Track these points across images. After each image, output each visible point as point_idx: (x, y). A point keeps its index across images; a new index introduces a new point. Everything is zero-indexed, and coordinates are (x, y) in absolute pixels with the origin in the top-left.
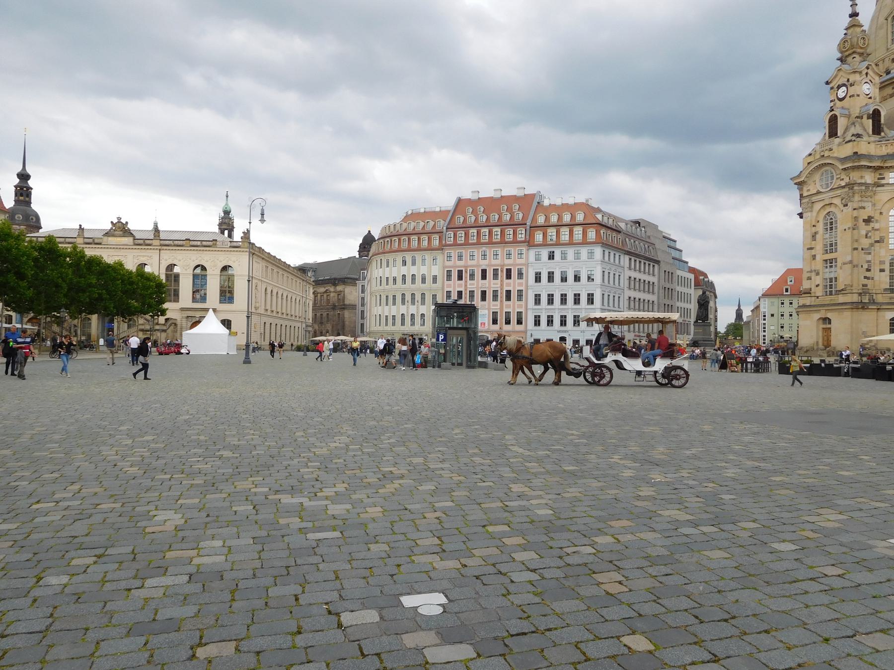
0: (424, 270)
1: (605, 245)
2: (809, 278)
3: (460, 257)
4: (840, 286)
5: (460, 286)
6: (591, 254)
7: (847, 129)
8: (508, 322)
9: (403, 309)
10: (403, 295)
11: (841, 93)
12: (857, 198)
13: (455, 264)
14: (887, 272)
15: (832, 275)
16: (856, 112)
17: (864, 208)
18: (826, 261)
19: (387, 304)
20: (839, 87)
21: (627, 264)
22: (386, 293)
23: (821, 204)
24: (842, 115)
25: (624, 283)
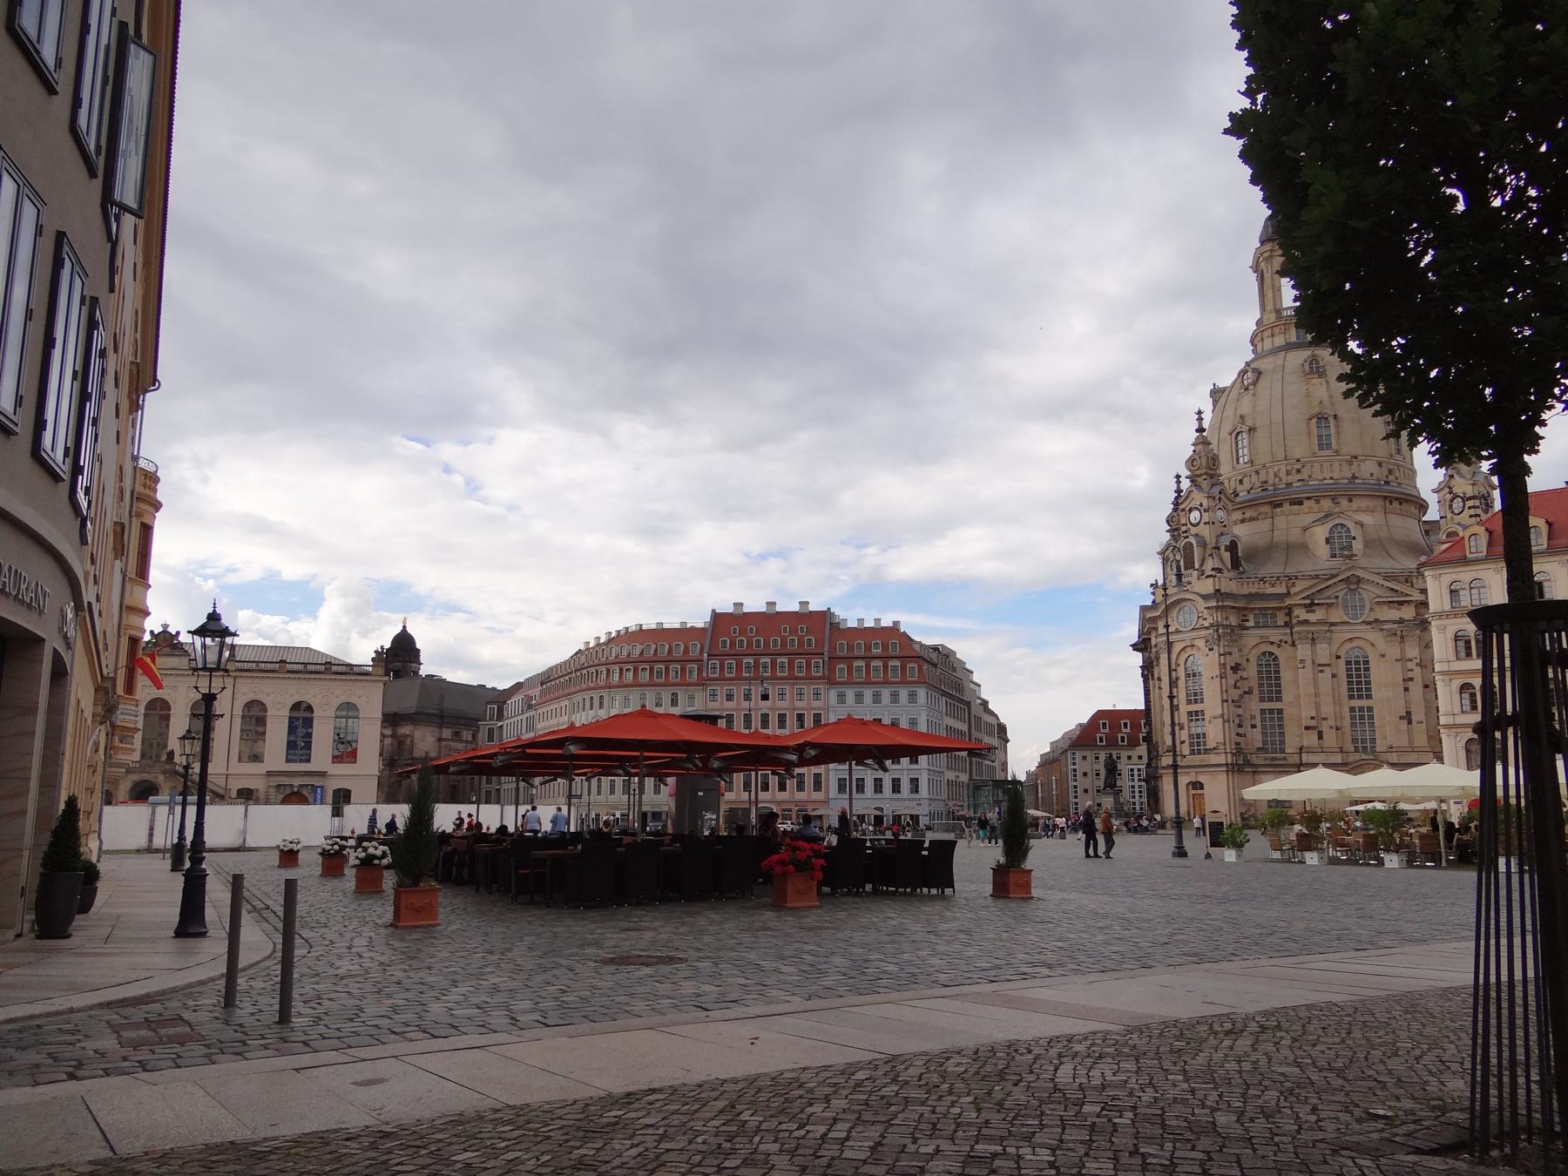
4: (1210, 745)
6: (913, 697)
11: (1195, 516)
14: (1259, 729)
15: (1199, 731)
16: (1211, 541)
18: (1190, 713)
23: (1182, 645)
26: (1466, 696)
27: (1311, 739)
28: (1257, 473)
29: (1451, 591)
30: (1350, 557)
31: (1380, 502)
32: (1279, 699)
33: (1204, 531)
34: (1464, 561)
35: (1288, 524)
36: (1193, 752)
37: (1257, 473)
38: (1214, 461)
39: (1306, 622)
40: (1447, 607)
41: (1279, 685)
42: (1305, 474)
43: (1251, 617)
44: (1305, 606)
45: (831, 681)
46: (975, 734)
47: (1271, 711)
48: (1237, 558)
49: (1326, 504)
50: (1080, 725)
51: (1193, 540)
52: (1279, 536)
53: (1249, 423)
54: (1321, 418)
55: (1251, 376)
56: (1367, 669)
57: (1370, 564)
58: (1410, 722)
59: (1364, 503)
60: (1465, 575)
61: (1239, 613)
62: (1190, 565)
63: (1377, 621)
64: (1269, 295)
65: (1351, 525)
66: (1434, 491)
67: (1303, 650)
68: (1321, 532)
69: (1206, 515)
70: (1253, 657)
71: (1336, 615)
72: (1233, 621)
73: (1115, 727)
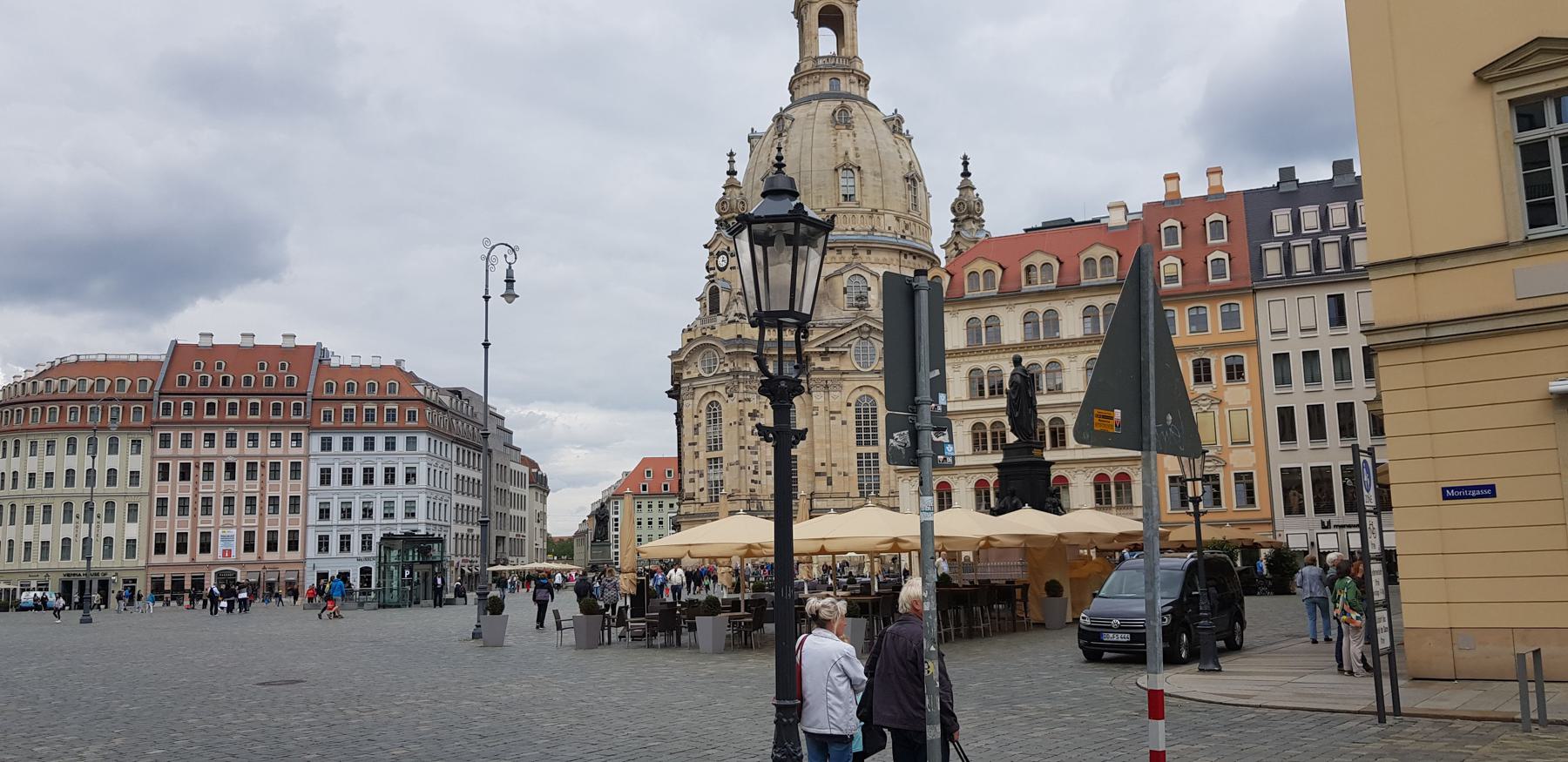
0: (113, 461)
1: (430, 430)
2: (692, 481)
3: (186, 442)
5: (186, 489)
6: (411, 443)
8: (272, 546)
9: (67, 530)
10: (68, 505)
11: (722, 261)
12: (742, 388)
13: (176, 453)
15: (718, 478)
19: (29, 522)
20: (719, 254)
22: (28, 502)
24: (725, 289)
27: (821, 485)
31: (896, 256)
44: (821, 354)
45: (312, 429)
49: (847, 255)
56: (875, 417)
62: (714, 309)
65: (867, 276)
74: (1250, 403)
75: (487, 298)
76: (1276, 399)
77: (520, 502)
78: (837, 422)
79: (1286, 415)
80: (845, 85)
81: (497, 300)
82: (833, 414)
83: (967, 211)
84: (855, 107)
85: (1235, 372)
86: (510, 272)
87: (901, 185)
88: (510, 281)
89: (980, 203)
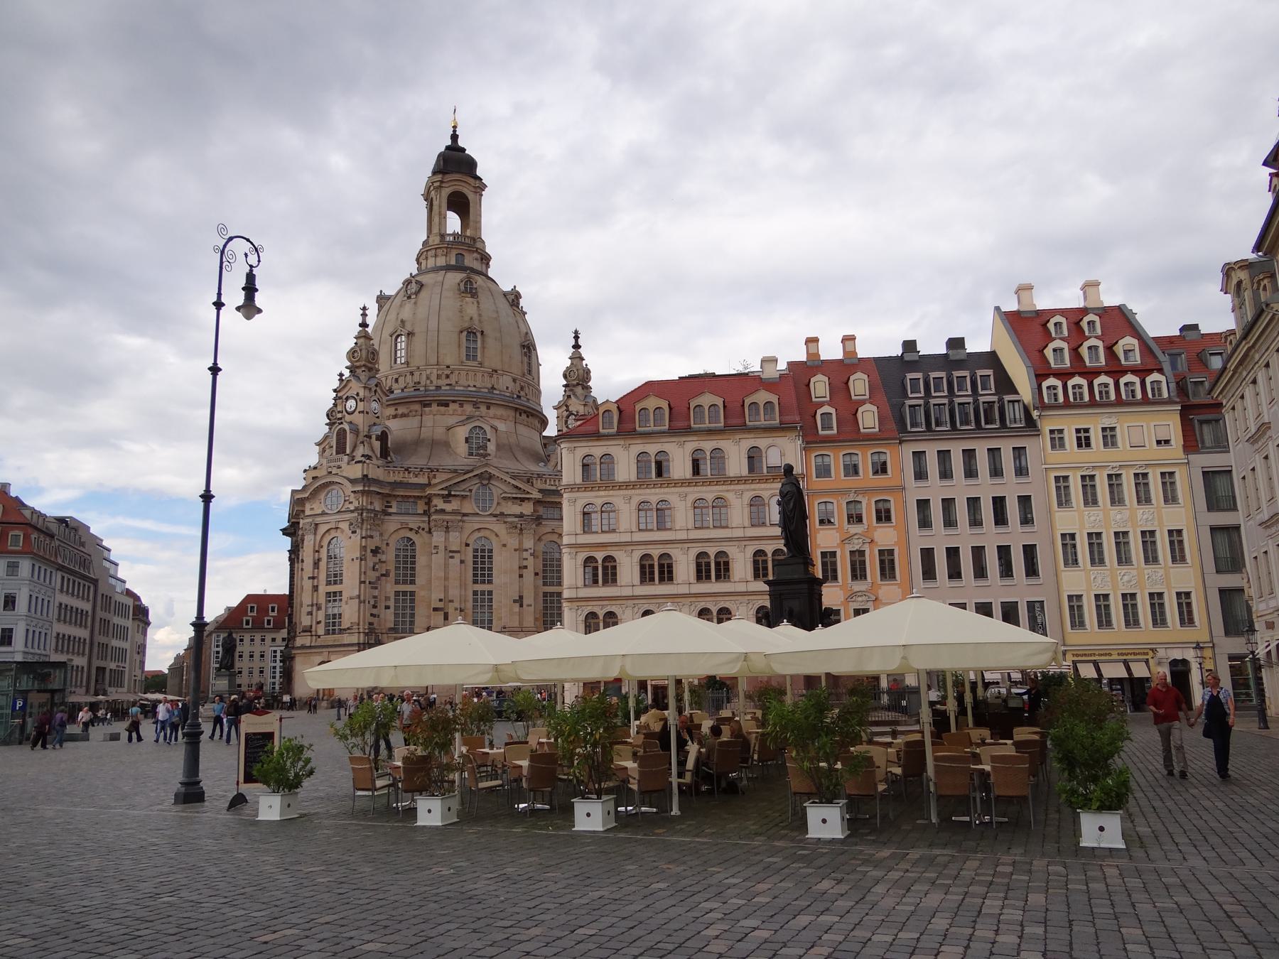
1: (36, 557)
2: (310, 613)
4: (345, 625)
7: (354, 448)
14: (392, 610)
15: (336, 611)
16: (363, 429)
17: (371, 537)
18: (328, 594)
20: (347, 399)
21: (58, 586)
25: (54, 612)
26: (589, 570)
28: (412, 374)
29: (584, 465)
30: (485, 456)
31: (512, 413)
32: (413, 582)
33: (358, 419)
34: (596, 436)
35: (435, 422)
36: (327, 633)
37: (412, 374)
38: (374, 354)
39: (443, 511)
40: (579, 480)
41: (413, 569)
42: (453, 380)
43: (394, 504)
44: (443, 496)
46: (100, 614)
47: (405, 593)
48: (386, 449)
49: (469, 408)
50: (229, 609)
51: (346, 427)
52: (426, 433)
53: (409, 328)
54: (471, 333)
55: (413, 287)
56: (490, 557)
57: (501, 464)
58: (521, 606)
59: (500, 412)
60: (597, 450)
61: (380, 499)
63: (502, 514)
64: (436, 219)
65: (487, 428)
66: (555, 408)
67: (438, 538)
68: (462, 432)
69: (361, 405)
70: (392, 542)
71: (468, 507)
72: (378, 506)
73: (263, 611)
74: (896, 543)
75: (219, 305)
76: (919, 539)
77: (122, 633)
78: (456, 561)
79: (927, 555)
80: (470, 261)
81: (230, 316)
82: (451, 553)
83: (577, 378)
84: (479, 280)
85: (883, 516)
86: (251, 278)
87: (517, 352)
88: (250, 289)
89: (588, 372)
